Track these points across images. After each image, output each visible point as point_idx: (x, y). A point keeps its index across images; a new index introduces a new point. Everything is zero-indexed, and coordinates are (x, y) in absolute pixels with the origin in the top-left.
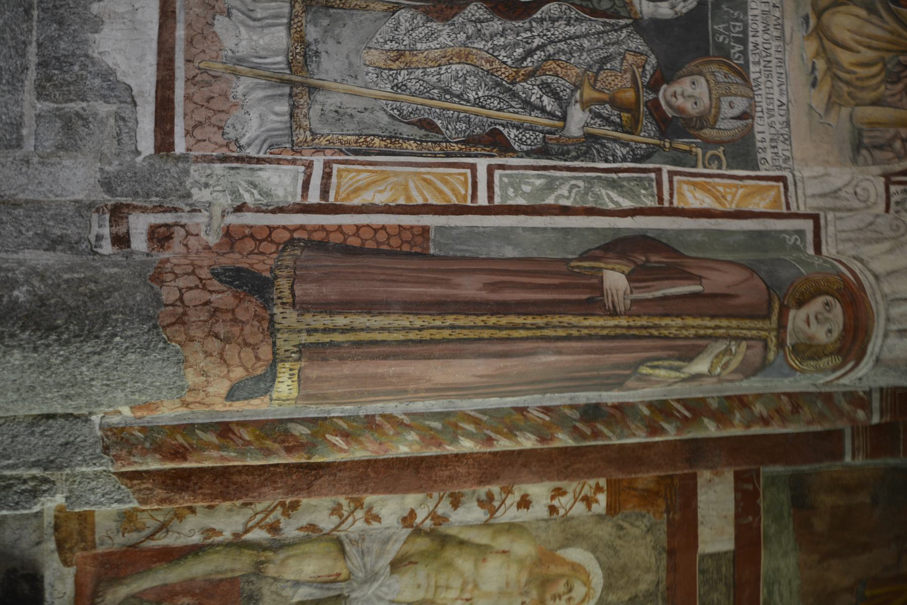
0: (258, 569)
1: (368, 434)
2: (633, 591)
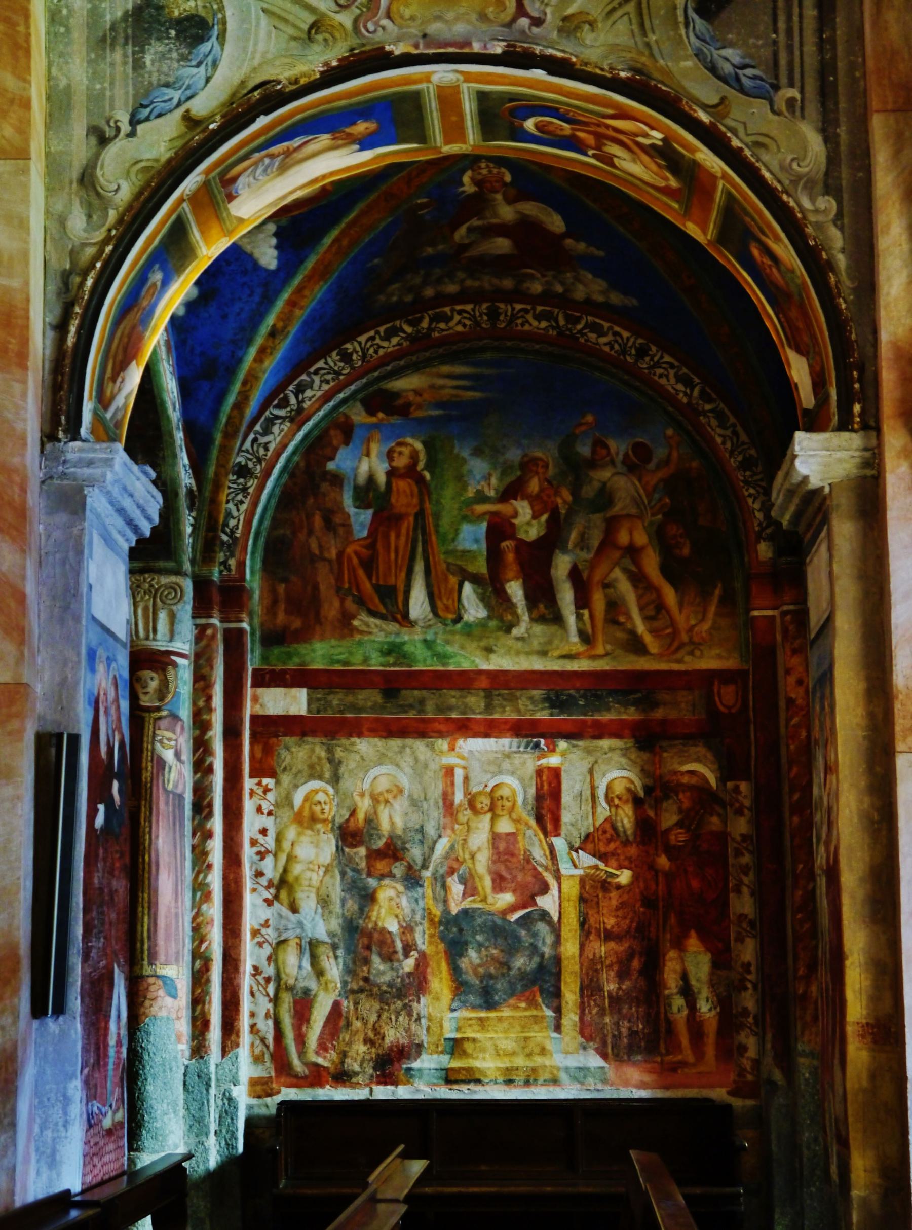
0: (290, 989)
1: (202, 930)
2: (324, 761)
